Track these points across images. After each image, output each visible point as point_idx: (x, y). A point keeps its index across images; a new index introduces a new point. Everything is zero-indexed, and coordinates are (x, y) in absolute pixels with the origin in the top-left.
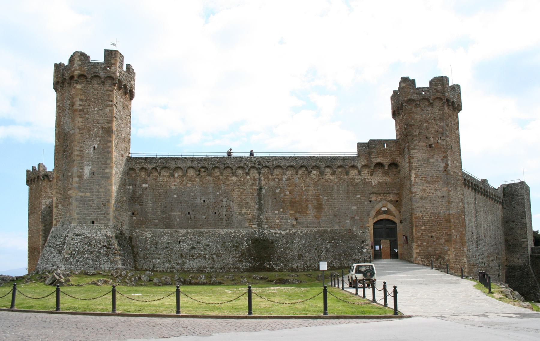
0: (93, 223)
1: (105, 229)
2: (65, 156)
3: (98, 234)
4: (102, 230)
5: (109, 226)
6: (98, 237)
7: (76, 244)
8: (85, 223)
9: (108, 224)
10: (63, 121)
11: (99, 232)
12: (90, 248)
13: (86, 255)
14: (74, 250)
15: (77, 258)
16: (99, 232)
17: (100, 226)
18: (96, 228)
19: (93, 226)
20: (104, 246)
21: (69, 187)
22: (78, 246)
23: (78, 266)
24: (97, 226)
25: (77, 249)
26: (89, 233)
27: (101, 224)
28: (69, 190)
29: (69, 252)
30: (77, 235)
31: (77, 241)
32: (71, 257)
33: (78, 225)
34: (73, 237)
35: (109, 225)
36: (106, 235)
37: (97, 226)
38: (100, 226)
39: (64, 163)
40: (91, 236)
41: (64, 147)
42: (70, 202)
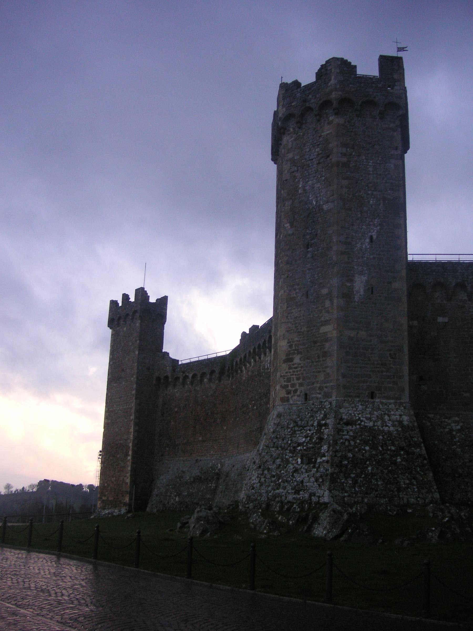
0: (372, 395)
1: (397, 410)
2: (309, 255)
3: (385, 422)
4: (392, 413)
5: (403, 403)
6: (386, 429)
7: (347, 443)
8: (358, 397)
9: (400, 399)
10: (304, 187)
11: (386, 417)
12: (374, 452)
13: (370, 468)
14: (346, 457)
15: (353, 476)
16: (386, 417)
17: (386, 404)
18: (379, 409)
19: (374, 402)
20: (402, 449)
21: (322, 319)
22: (351, 448)
23: (356, 493)
24: (382, 403)
25: (350, 455)
26: (369, 419)
27: (389, 398)
28: (322, 325)
29: (336, 460)
30: (347, 424)
31: (347, 437)
32: (340, 472)
33: (345, 400)
34: (339, 426)
35: (402, 401)
36: (400, 422)
37: (382, 403)
38: (386, 404)
39: (309, 269)
40: (374, 426)
41: (308, 237)
42: (326, 349)
